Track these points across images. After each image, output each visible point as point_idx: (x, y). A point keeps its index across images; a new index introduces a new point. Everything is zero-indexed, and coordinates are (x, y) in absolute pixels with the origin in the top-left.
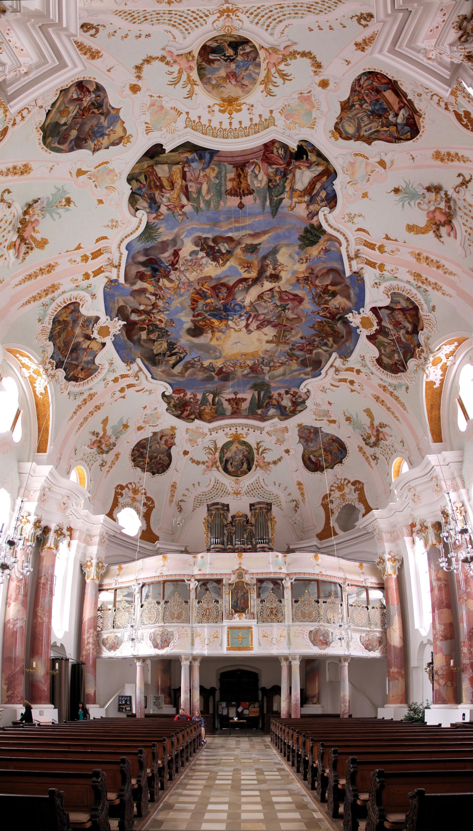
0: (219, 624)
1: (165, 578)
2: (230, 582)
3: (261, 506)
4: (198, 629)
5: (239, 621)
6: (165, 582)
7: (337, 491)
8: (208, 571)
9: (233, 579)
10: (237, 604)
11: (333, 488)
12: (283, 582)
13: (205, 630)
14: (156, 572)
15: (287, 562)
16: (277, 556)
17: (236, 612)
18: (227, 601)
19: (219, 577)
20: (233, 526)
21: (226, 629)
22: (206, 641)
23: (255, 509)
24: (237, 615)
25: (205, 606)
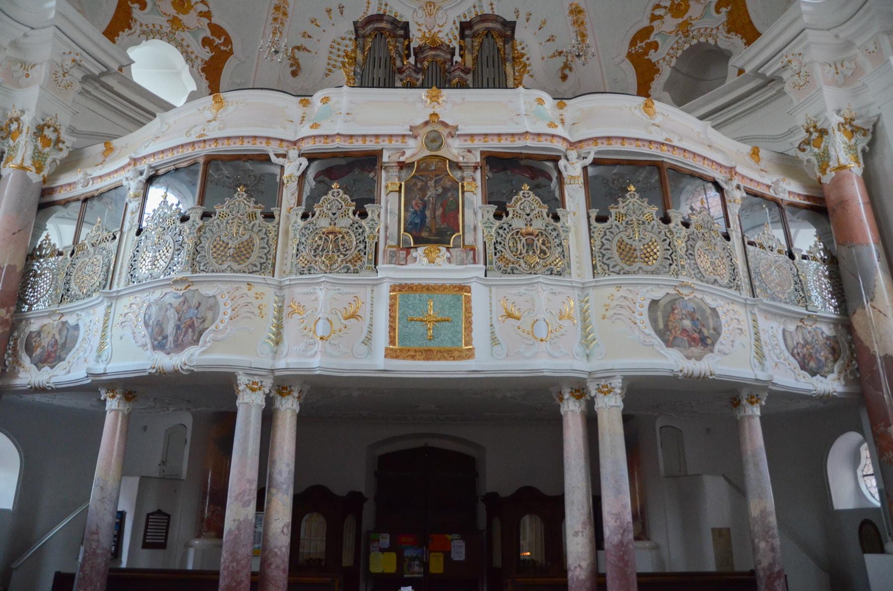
0: (365, 276)
1: (211, 149)
2: (402, 159)
3: (490, 25)
4: (298, 290)
5: (429, 266)
6: (211, 160)
7: (668, 17)
8: (340, 127)
9: (414, 150)
10: (423, 218)
11: (658, 12)
12: (562, 163)
13: (322, 296)
14: (188, 133)
15: (568, 121)
16: (540, 101)
17: (419, 241)
18: (389, 211)
19: (370, 145)
20: (417, 71)
21: (385, 291)
22: (319, 324)
23: (474, 36)
24: (421, 250)
25: (324, 223)
